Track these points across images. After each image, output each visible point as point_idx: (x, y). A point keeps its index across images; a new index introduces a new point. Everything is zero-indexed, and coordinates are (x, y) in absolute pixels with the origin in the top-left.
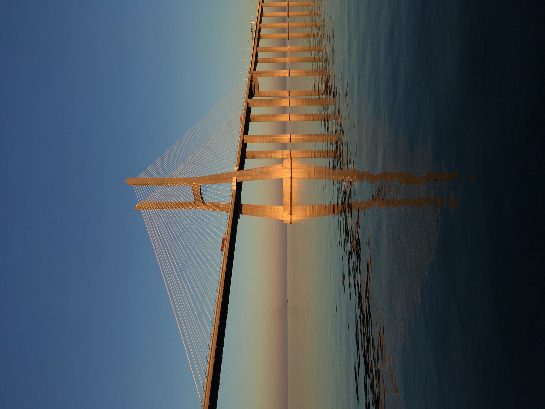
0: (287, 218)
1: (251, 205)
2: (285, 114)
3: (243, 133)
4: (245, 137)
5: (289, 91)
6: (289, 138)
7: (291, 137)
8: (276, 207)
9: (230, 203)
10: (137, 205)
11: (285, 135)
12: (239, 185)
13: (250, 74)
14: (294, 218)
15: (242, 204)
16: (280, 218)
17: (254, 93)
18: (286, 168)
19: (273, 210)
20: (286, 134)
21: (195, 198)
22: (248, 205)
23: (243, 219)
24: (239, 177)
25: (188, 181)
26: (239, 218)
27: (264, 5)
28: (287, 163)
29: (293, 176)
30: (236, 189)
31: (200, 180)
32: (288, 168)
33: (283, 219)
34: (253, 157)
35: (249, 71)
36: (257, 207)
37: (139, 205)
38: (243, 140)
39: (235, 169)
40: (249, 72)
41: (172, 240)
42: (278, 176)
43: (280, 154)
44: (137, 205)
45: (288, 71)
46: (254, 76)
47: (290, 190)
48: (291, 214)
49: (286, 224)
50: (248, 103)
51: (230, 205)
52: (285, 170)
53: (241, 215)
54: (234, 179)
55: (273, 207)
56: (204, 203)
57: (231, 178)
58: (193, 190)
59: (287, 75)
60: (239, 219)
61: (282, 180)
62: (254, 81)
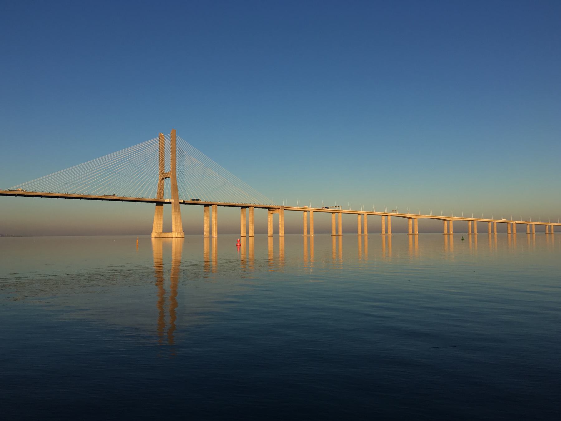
0: (153, 236)
1: (163, 211)
2: (246, 233)
4: (215, 206)
5: (272, 236)
6: (215, 236)
7: (215, 238)
8: (162, 228)
10: (162, 134)
11: (217, 233)
12: (170, 203)
14: (153, 239)
15: (163, 205)
16: (153, 231)
17: (270, 210)
18: (177, 234)
19: (159, 225)
20: (218, 234)
22: (163, 209)
24: (174, 203)
25: (174, 168)
27: (365, 215)
28: (179, 236)
29: (173, 239)
30: (166, 201)
31: (174, 177)
32: (177, 236)
33: (153, 233)
34: (205, 211)
35: (284, 206)
36: (161, 215)
37: (162, 136)
38: (214, 205)
39: (181, 201)
40: (283, 207)
41: (131, 162)
42: (174, 229)
43: (206, 230)
44: (162, 134)
45: (283, 235)
46: (280, 210)
48: (155, 238)
49: (151, 235)
50: (251, 207)
54: (172, 201)
55: (162, 226)
56: (163, 179)
57: (173, 198)
58: (168, 173)
59: (280, 235)
61: (171, 231)
62: (277, 210)
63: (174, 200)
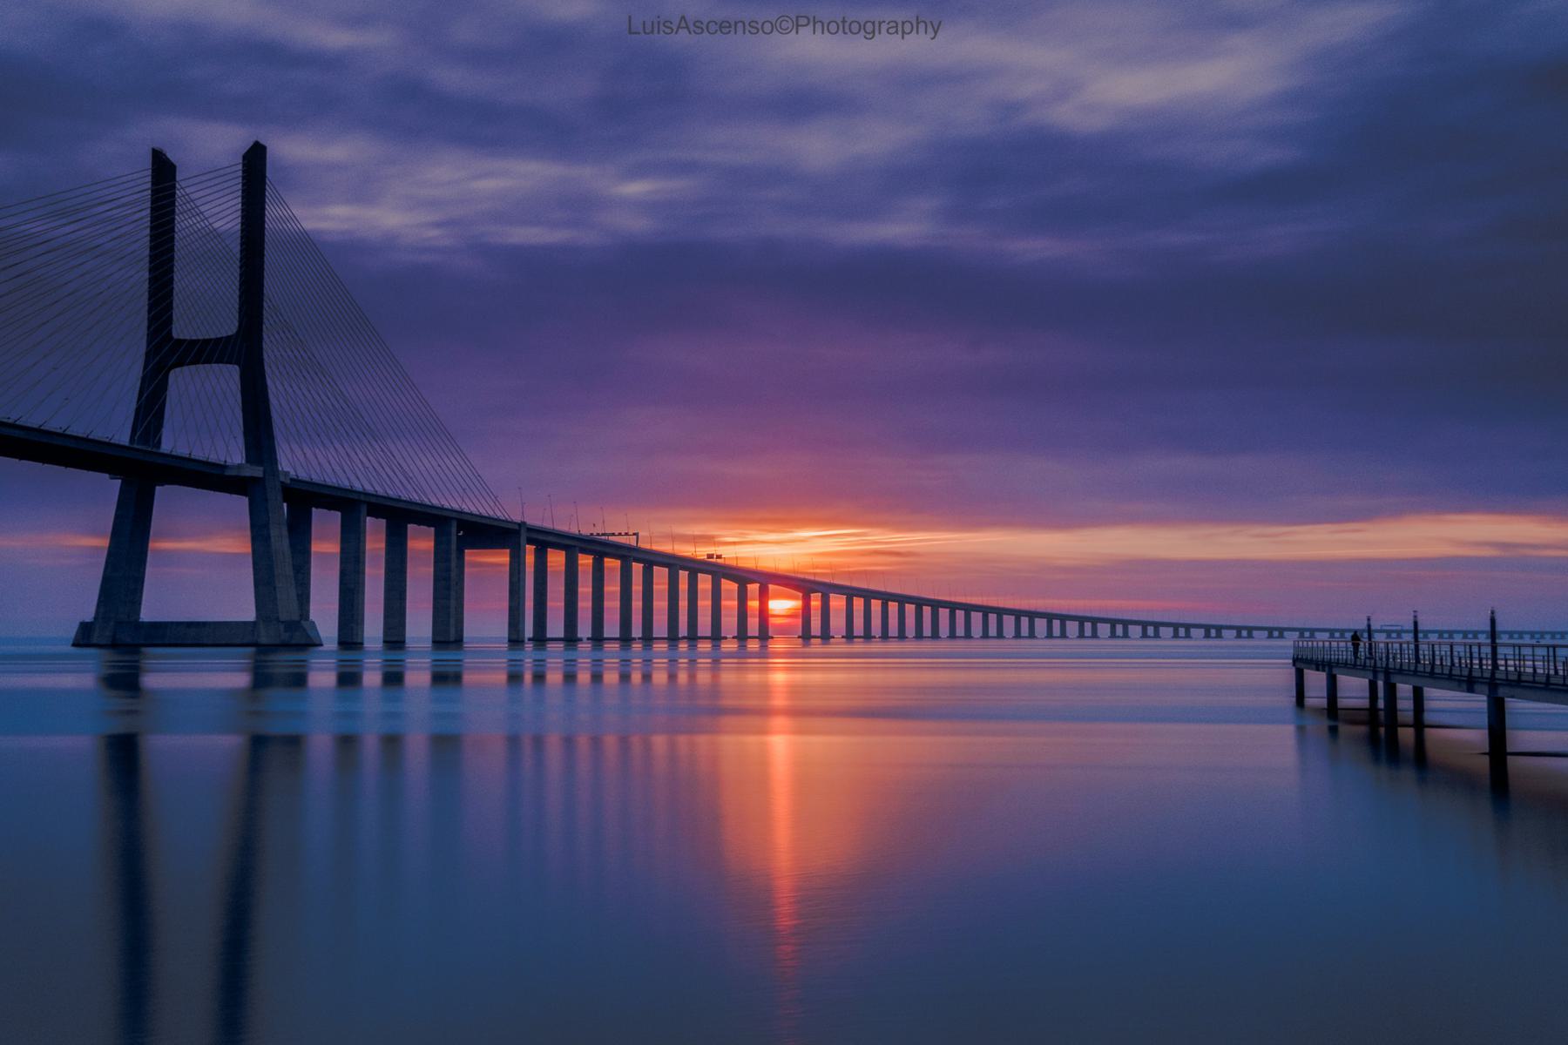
3: (373, 500)
9: (161, 451)
13: (517, 527)
21: (181, 342)
23: (107, 489)
26: (112, 478)
35: (524, 523)
47: (210, 642)
51: (154, 450)
52: (282, 627)
53: (120, 481)
54: (257, 472)
60: (107, 475)
63: (264, 472)
